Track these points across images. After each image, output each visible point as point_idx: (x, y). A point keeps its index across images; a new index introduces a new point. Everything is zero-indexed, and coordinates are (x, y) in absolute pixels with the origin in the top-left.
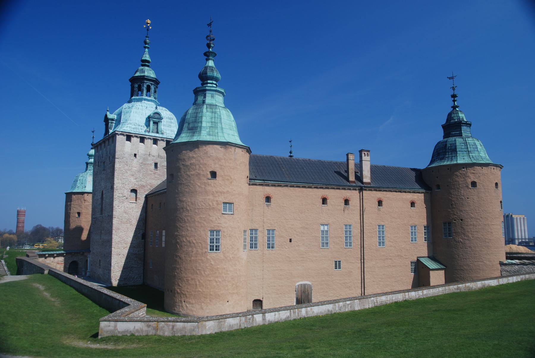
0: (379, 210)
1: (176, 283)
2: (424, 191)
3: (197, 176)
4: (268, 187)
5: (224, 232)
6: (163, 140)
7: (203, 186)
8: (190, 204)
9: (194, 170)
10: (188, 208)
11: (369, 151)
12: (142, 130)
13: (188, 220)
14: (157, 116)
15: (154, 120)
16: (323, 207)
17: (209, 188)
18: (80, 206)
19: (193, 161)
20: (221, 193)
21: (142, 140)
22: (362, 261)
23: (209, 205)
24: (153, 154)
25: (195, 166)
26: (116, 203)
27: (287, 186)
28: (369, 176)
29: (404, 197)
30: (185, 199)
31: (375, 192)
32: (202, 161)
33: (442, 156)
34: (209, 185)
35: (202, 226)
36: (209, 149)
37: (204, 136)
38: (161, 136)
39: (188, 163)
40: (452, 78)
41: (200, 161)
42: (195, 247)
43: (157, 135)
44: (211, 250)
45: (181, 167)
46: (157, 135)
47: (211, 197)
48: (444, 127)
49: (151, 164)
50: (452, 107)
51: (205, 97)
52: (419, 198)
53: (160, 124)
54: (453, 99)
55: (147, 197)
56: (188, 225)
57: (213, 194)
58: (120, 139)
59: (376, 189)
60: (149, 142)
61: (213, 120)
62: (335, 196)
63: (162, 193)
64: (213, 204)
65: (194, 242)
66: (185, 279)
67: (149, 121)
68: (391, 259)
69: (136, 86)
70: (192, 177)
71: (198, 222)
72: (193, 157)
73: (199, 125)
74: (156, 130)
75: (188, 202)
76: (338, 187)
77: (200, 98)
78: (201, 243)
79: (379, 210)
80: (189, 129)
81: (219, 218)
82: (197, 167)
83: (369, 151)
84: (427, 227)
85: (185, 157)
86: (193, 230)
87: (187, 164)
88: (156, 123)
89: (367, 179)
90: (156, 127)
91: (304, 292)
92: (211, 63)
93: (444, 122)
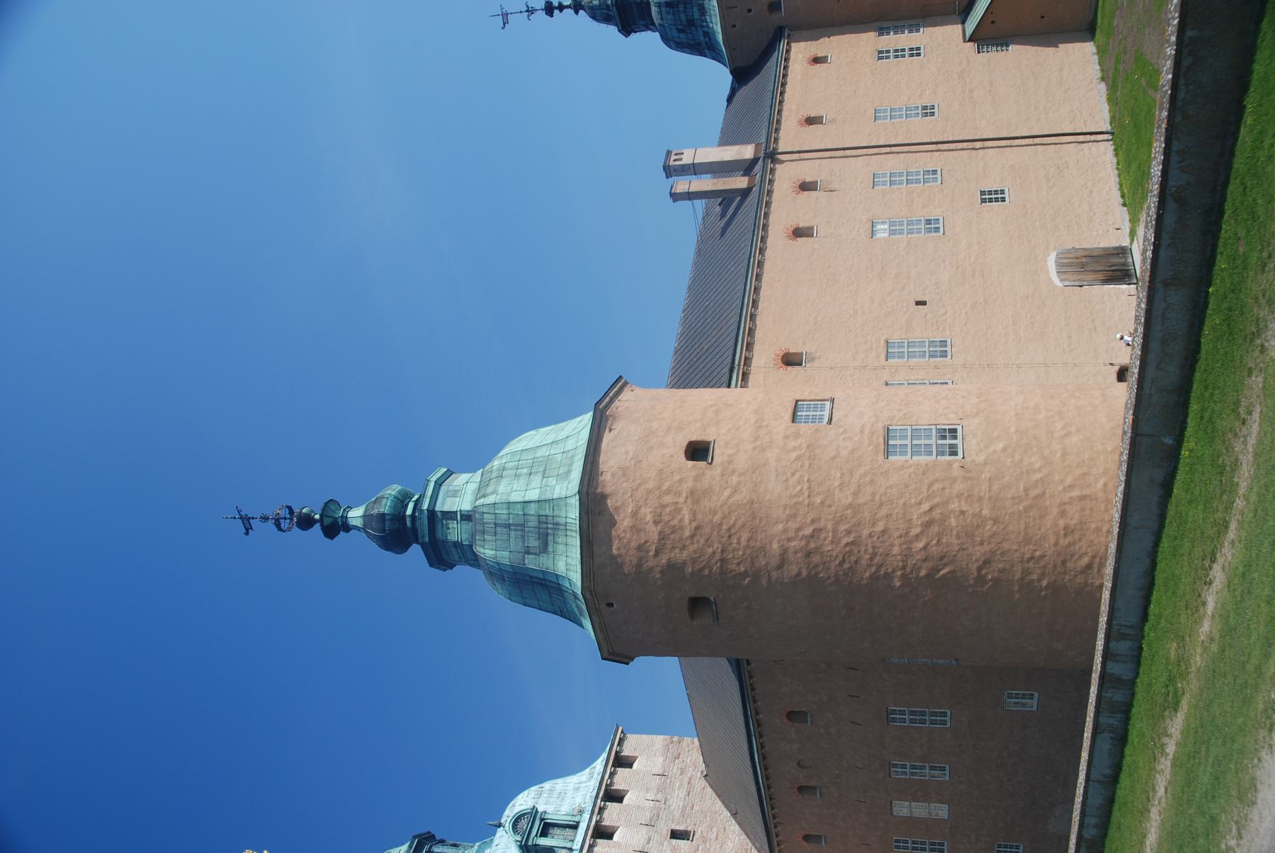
0: (833, 121)
1: (1080, 579)
2: (783, 45)
3: (697, 501)
4: (755, 363)
5: (892, 418)
6: (601, 810)
7: (735, 479)
8: (793, 525)
9: (678, 510)
10: (808, 531)
11: (669, 153)
13: (848, 532)
14: (523, 824)
16: (821, 233)
17: (742, 462)
19: (647, 514)
20: (759, 427)
22: (978, 145)
23: (798, 458)
24: (643, 841)
25: (663, 506)
27: (753, 317)
28: (736, 148)
29: (799, 77)
30: (775, 546)
31: (782, 133)
32: (650, 485)
33: (696, 10)
34: (730, 462)
35: (872, 482)
36: (612, 463)
37: (567, 487)
38: (586, 816)
39: (653, 533)
40: (505, 16)
41: (649, 492)
42: (947, 502)
43: (583, 826)
44: (954, 453)
45: (664, 559)
46: (583, 826)
47: (772, 455)
48: (627, 30)
49: (674, 849)
50: (577, 13)
51: (450, 515)
52: (800, 52)
53: (552, 817)
54: (556, 12)
56: (865, 533)
57: (764, 450)
59: (774, 126)
61: (525, 471)
62: (785, 208)
63: (763, 757)
64: (794, 449)
65: (926, 507)
66: (1063, 542)
68: (971, 91)
70: (700, 517)
71: (855, 494)
72: (635, 514)
73: (532, 509)
74: (569, 832)
75: (785, 531)
76: (765, 204)
78: (931, 485)
79: (833, 121)
80: (544, 548)
81: (845, 432)
82: (668, 499)
83: (669, 153)
84: (882, 31)
85: (634, 544)
86: (884, 512)
87: (656, 538)
89: (748, 152)
90: (557, 831)
91: (1083, 266)
92: (356, 515)
93: (612, 30)
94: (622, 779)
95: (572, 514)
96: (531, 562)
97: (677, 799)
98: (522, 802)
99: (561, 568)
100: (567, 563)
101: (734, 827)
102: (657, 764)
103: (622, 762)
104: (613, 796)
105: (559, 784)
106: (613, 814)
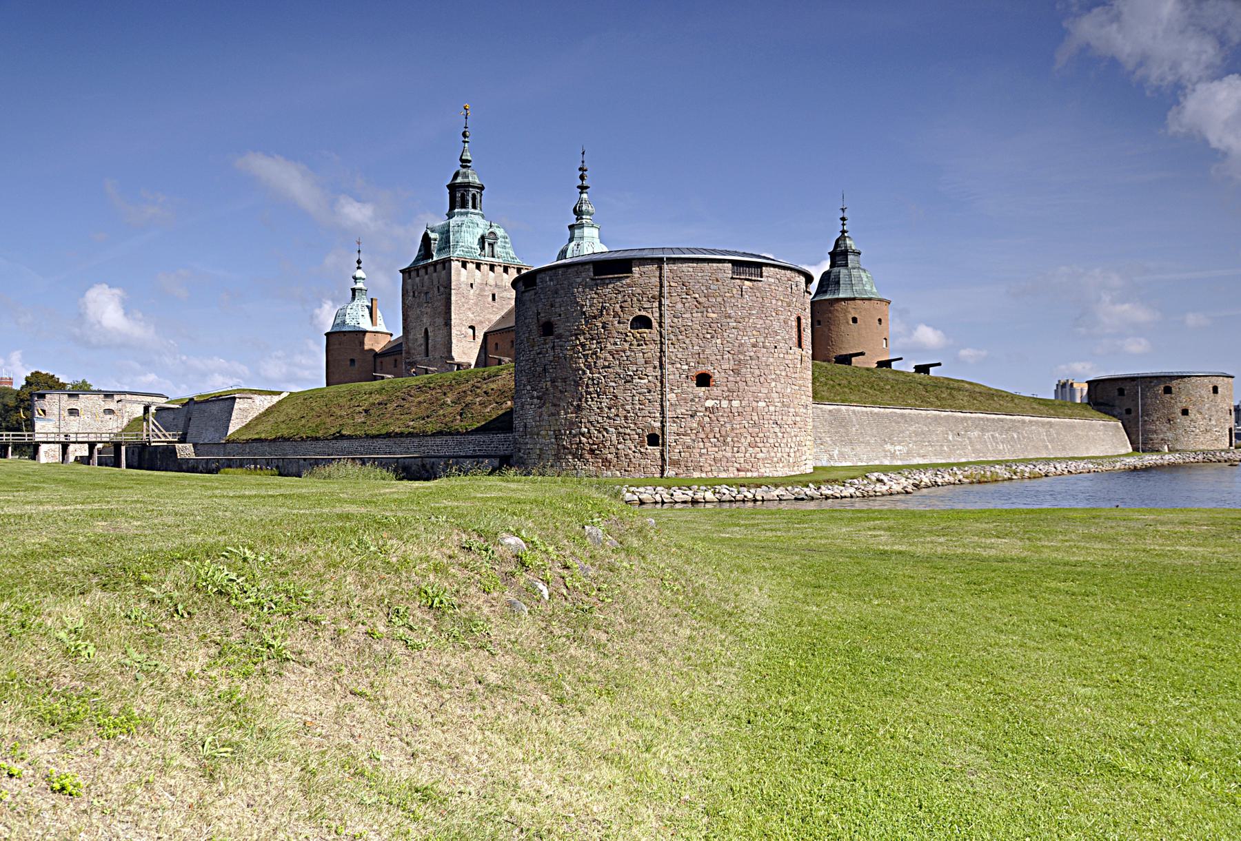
21: (478, 266)
55: (486, 335)
58: (456, 265)
60: (485, 268)
67: (483, 243)
69: (458, 195)
77: (577, 232)
88: (491, 245)
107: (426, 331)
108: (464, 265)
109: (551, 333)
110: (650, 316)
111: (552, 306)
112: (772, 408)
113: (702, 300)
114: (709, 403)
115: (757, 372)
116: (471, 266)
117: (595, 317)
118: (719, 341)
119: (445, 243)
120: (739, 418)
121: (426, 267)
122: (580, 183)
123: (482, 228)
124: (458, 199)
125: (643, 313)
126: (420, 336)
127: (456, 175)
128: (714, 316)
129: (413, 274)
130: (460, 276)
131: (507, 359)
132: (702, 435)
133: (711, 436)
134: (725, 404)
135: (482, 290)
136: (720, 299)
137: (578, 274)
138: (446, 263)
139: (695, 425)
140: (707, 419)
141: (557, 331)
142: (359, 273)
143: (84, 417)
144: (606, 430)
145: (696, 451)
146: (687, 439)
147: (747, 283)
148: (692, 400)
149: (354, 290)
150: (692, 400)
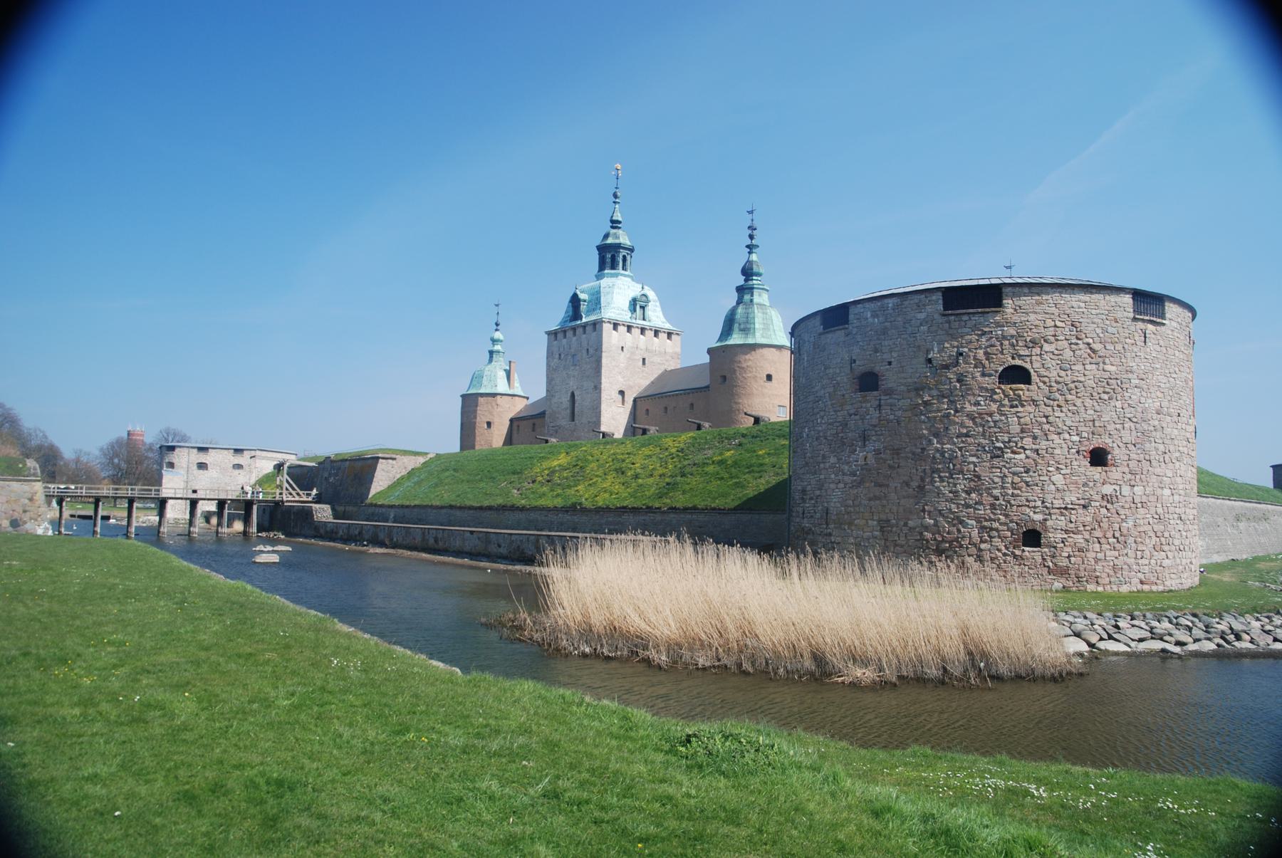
12: (626, 316)
15: (637, 305)
18: (491, 413)
19: (750, 363)
21: (629, 328)
26: (603, 407)
39: (744, 365)
40: (1009, 267)
55: (635, 400)
58: (607, 328)
60: (636, 332)
67: (635, 305)
69: (609, 256)
77: (747, 297)
88: (643, 308)
92: (754, 257)
94: (663, 336)
95: (750, 341)
96: (736, 326)
97: (657, 359)
98: (651, 295)
99: (735, 336)
100: (736, 339)
101: (648, 382)
102: (669, 350)
103: (669, 335)
104: (656, 333)
105: (659, 309)
106: (650, 334)
107: (573, 395)
108: (615, 326)
109: (875, 387)
110: (1028, 366)
111: (876, 351)
112: (1176, 498)
113: (1096, 346)
114: (1108, 489)
115: (1161, 447)
116: (622, 329)
117: (947, 367)
118: (1119, 404)
119: (596, 303)
120: (1141, 511)
121: (574, 329)
122: (749, 242)
123: (634, 290)
124: (608, 260)
125: (1018, 362)
126: (566, 399)
127: (606, 236)
128: (1113, 369)
129: (560, 336)
130: (611, 339)
131: (707, 425)
132: (1098, 533)
133: (1109, 534)
134: (1126, 490)
135: (633, 353)
136: (1119, 347)
137: (920, 307)
138: (597, 325)
139: (1089, 519)
140: (1104, 511)
141: (884, 385)
142: (498, 335)
143: (212, 473)
144: (961, 522)
145: (1091, 555)
146: (1079, 539)
147: (1150, 326)
148: (1085, 485)
149: (491, 353)
150: (1085, 485)
